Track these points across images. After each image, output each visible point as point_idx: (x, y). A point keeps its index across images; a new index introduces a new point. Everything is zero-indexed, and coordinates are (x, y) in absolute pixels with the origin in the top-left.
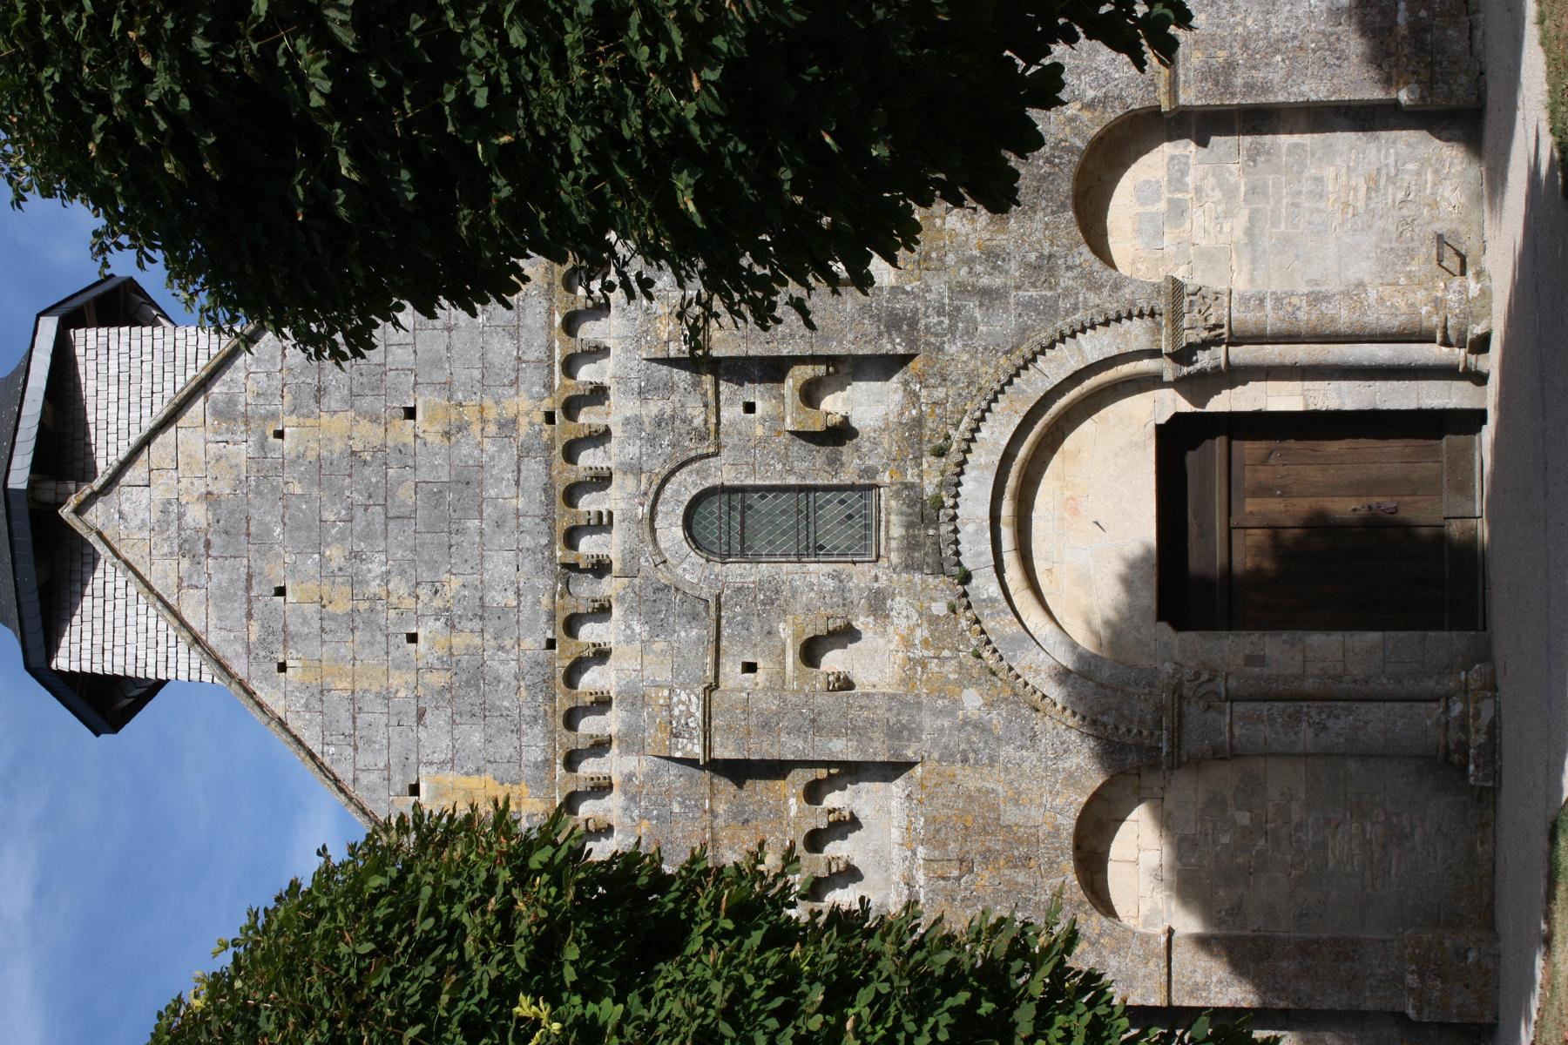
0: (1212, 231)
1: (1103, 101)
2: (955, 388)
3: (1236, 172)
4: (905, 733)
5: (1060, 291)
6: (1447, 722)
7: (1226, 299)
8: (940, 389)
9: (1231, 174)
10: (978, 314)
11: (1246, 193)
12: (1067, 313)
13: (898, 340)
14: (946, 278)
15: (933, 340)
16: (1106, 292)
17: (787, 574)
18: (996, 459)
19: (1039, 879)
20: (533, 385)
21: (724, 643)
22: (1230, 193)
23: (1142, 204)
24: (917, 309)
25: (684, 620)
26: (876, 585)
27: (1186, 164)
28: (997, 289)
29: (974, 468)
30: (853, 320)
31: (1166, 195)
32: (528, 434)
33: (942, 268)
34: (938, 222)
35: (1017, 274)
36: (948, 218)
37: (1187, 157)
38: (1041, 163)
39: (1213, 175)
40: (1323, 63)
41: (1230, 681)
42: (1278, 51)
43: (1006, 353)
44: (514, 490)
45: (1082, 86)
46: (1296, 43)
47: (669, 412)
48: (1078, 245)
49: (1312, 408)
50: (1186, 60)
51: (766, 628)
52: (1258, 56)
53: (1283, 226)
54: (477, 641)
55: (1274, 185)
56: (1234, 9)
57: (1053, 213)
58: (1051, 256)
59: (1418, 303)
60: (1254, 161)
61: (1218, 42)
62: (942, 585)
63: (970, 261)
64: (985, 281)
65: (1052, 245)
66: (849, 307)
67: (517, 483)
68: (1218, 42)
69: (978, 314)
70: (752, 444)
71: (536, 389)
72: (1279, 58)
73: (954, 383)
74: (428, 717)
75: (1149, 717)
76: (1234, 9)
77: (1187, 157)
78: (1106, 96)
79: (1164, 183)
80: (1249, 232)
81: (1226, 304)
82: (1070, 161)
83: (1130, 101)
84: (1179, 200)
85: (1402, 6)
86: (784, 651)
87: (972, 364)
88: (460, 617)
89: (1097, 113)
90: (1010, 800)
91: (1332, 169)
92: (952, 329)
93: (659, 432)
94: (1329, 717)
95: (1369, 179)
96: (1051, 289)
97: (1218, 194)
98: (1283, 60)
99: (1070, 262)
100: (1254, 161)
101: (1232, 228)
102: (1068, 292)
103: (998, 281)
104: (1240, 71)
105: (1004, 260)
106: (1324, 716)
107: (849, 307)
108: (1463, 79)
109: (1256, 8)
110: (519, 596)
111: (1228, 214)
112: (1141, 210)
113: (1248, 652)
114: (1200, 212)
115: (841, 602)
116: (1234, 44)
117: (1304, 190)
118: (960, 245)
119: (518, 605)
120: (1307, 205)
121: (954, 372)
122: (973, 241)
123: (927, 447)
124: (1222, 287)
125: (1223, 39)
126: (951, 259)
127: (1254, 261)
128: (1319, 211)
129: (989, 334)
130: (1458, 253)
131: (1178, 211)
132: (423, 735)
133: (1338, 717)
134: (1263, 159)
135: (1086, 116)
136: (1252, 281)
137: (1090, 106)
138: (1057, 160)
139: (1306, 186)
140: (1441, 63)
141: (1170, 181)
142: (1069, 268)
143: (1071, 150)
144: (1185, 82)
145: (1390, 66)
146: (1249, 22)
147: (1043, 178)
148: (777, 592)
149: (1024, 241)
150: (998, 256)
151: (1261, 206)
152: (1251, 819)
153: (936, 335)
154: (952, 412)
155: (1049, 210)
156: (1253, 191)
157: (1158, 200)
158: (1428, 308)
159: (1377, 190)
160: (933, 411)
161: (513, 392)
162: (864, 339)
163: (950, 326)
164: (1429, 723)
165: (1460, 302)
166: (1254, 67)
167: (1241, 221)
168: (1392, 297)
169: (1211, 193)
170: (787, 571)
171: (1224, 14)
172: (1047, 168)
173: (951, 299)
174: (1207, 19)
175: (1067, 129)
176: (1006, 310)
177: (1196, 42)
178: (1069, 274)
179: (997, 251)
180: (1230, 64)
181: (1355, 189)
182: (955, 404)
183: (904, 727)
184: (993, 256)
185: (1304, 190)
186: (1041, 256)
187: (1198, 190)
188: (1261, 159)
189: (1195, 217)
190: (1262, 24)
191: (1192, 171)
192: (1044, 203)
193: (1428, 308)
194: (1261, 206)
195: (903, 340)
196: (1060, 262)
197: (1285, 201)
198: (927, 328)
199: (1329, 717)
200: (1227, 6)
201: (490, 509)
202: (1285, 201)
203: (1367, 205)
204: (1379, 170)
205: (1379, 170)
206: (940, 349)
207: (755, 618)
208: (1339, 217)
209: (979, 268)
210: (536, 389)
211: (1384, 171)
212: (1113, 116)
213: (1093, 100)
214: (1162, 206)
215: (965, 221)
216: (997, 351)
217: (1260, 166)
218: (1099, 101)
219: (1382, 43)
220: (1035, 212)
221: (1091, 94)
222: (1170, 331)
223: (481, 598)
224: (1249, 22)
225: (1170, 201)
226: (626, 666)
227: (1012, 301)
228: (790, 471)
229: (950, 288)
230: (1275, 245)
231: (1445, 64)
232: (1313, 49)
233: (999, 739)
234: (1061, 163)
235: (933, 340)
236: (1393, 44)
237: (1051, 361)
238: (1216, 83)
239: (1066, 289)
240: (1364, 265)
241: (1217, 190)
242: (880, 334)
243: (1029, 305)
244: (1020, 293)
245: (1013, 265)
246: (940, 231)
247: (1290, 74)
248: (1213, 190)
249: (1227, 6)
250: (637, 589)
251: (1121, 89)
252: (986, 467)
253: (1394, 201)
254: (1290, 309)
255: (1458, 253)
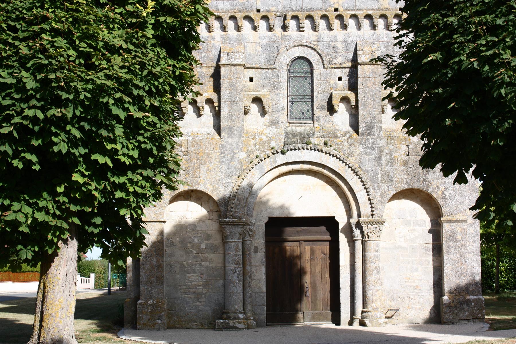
1: (444, 198)
2: (347, 149)
4: (230, 133)
5: (380, 184)
8: (347, 143)
10: (373, 156)
11: (413, 246)
13: (363, 129)
15: (364, 141)
16: (380, 199)
17: (283, 92)
20: (348, 4)
21: (260, 70)
25: (267, 57)
26: (280, 122)
28: (381, 163)
30: (370, 114)
33: (388, 144)
34: (404, 143)
35: (386, 169)
37: (425, 226)
38: (424, 177)
40: (457, 271)
41: (249, 241)
42: (461, 256)
43: (359, 166)
45: (449, 191)
46: (464, 262)
47: (338, 51)
48: (396, 190)
49: (341, 268)
51: (265, 85)
57: (407, 181)
59: (376, 303)
60: (423, 249)
61: (464, 236)
62: (280, 144)
64: (384, 159)
65: (396, 181)
66: (375, 112)
68: (464, 236)
69: (373, 156)
70: (328, 80)
72: (459, 256)
73: (349, 148)
75: (237, 214)
77: (425, 226)
81: (376, 239)
82: (424, 187)
83: (444, 207)
86: (257, 91)
87: (355, 154)
89: (440, 196)
92: (367, 148)
93: (332, 48)
94: (238, 274)
96: (381, 181)
99: (390, 187)
100: (423, 249)
103: (384, 163)
104: (454, 244)
105: (391, 165)
106: (238, 272)
107: (375, 112)
108: (451, 317)
109: (475, 249)
113: (259, 247)
115: (274, 110)
118: (396, 150)
121: (353, 149)
122: (397, 154)
124: (381, 238)
125: (465, 238)
126: (391, 147)
129: (366, 160)
130: (392, 316)
131: (407, 223)
133: (238, 277)
135: (440, 192)
137: (443, 194)
138: (424, 183)
140: (456, 310)
142: (388, 187)
143: (428, 187)
144: (451, 225)
145: (456, 293)
147: (418, 178)
150: (392, 163)
153: (365, 142)
154: (339, 148)
155: (408, 180)
159: (414, 289)
160: (339, 141)
163: (368, 147)
164: (236, 307)
166: (455, 248)
170: (284, 92)
171: (473, 238)
172: (422, 179)
173: (378, 147)
174: (471, 233)
175: (435, 186)
177: (464, 229)
178: (386, 187)
179: (394, 163)
183: (232, 132)
184: (392, 161)
185: (414, 265)
186: (392, 177)
187: (414, 230)
188: (424, 251)
190: (470, 251)
192: (410, 178)
195: (363, 131)
196: (390, 184)
198: (368, 139)
199: (238, 274)
204: (420, 290)
205: (420, 290)
206: (360, 143)
207: (268, 81)
209: (388, 156)
210: (346, 5)
212: (439, 201)
216: (360, 163)
217: (422, 250)
219: (463, 290)
222: (367, 221)
224: (470, 247)
226: (251, 37)
227: (377, 168)
229: (381, 147)
231: (456, 311)
233: (229, 164)
234: (423, 184)
235: (364, 141)
236: (463, 294)
238: (450, 236)
239: (381, 186)
242: (366, 123)
243: (375, 173)
246: (401, 143)
247: (453, 260)
250: (278, 40)
251: (448, 204)
253: (410, 295)
254: (374, 261)
255: (392, 316)
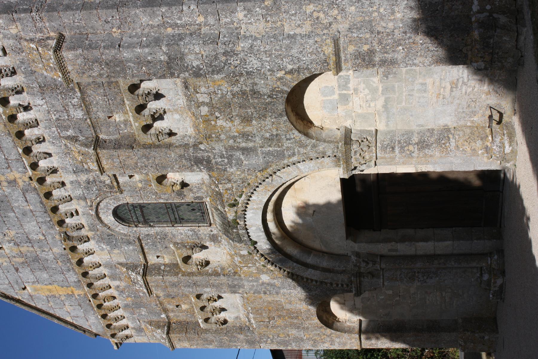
0: (364, 106)
1: (298, 70)
2: (236, 184)
3: (377, 82)
4: (237, 287)
5: (284, 148)
6: (481, 281)
7: (374, 149)
8: (228, 184)
9: (374, 82)
10: (242, 157)
11: (382, 91)
12: (290, 156)
13: (202, 168)
14: (222, 144)
15: (220, 167)
16: (309, 148)
17: (168, 230)
18: (262, 206)
19: (303, 322)
20: (18, 168)
21: (146, 251)
22: (374, 91)
23: (325, 96)
24: (210, 156)
25: (125, 244)
26: (212, 233)
27: (348, 79)
28: (251, 148)
29: (250, 209)
30: (176, 160)
31: (337, 92)
32: (24, 185)
33: (219, 139)
34: (213, 123)
35: (260, 142)
36: (218, 121)
37: (349, 76)
38: (266, 97)
39: (364, 83)
40: (427, 50)
41: (382, 265)
42: (401, 45)
43: (260, 171)
44: (26, 204)
45: (284, 64)
46: (411, 41)
47: (91, 179)
48: (291, 130)
49: (419, 171)
50: (345, 49)
51: (164, 246)
52: (388, 47)
53: (404, 104)
54: (32, 249)
55: (398, 86)
56: (371, 4)
57: (275, 117)
58: (277, 135)
59: (477, 149)
60: (387, 77)
61: (364, 41)
62: (244, 246)
63: (234, 138)
64: (243, 145)
65: (277, 130)
66: (173, 156)
67: (26, 201)
68: (364, 41)
69: (242, 157)
70: (138, 189)
71: (20, 169)
72: (401, 48)
73: (235, 182)
74: (20, 270)
75: (346, 280)
76: (371, 4)
77: (349, 76)
78: (299, 68)
79: (336, 88)
80: (385, 107)
81: (374, 151)
82: (282, 97)
83: (313, 70)
84: (345, 94)
85: (476, 2)
86: (174, 252)
87: (243, 175)
88: (20, 242)
89: (295, 76)
90: (287, 303)
91: (431, 79)
92: (230, 163)
93: (89, 186)
94: (427, 278)
95: (452, 83)
96: (279, 147)
97: (367, 91)
98: (403, 49)
99: (288, 137)
100: (387, 77)
101: (375, 105)
102: (288, 149)
103: (251, 145)
104: (377, 55)
105: (252, 137)
106: (425, 278)
107: (173, 156)
108: (510, 60)
109: (386, 3)
110: (44, 236)
111: (374, 99)
112: (324, 98)
113: (389, 248)
114: (357, 99)
115: (197, 238)
116: (373, 41)
117: (416, 89)
118: (227, 132)
119: (46, 238)
120: (417, 95)
121: (234, 178)
122: (234, 129)
123: (226, 204)
124: (373, 129)
125: (367, 39)
126: (223, 137)
127: (388, 118)
128: (424, 97)
129: (249, 164)
130: (499, 112)
131: (344, 99)
132: (21, 275)
133: (431, 278)
134: (392, 76)
135: (289, 77)
136: (387, 125)
137: (291, 72)
138: (274, 96)
139: (417, 87)
140: (498, 53)
141: (339, 86)
142: (287, 139)
143: (282, 92)
144: (345, 60)
145: (467, 50)
146: (382, 10)
147: (269, 103)
148: (166, 236)
149: (261, 130)
150: (249, 135)
151: (391, 96)
152: (393, 293)
153: (222, 165)
154: (236, 192)
155: (274, 117)
156: (386, 90)
157: (334, 93)
158: (483, 151)
159: (457, 87)
160: (227, 192)
161: (9, 171)
162: (184, 168)
163: (228, 162)
164: (473, 280)
165: (500, 152)
166: (386, 53)
167: (380, 102)
168: (463, 145)
169: (363, 91)
170: (169, 230)
171: (366, 6)
172: (269, 100)
173: (226, 152)
174: (356, 9)
175: (279, 83)
176: (257, 155)
177: (350, 41)
178: (289, 141)
179: (248, 133)
180: (371, 51)
181: (444, 88)
182: (237, 189)
183: (236, 285)
184: (245, 136)
185: (416, 89)
186: (272, 135)
187: (356, 90)
188: (390, 76)
189: (354, 101)
190: (389, 11)
191: (351, 82)
192: (270, 114)
193: (483, 151)
194: (391, 96)
195: (205, 167)
196: (283, 137)
197: (404, 94)
198: (217, 163)
199: (427, 278)
200: (368, 2)
201: (17, 210)
202: (404, 94)
203: (451, 94)
204: (458, 80)
205: (458, 80)
206: (225, 170)
207: (158, 243)
208: (435, 100)
209: (239, 140)
210: (20, 169)
211: (461, 80)
212: (304, 77)
213: (292, 70)
214: (336, 97)
215: (227, 122)
216: (255, 171)
217: (390, 79)
218: (295, 71)
219: (463, 40)
220: (266, 118)
221: (290, 67)
222: (345, 166)
223: (27, 237)
224: (382, 10)
225: (340, 95)
226: (103, 257)
227: (259, 152)
228: (160, 198)
229: (225, 148)
230: (399, 111)
231: (500, 53)
232: (421, 44)
233: (279, 287)
234: (277, 97)
235: (220, 167)
236: (469, 40)
237: (284, 173)
238: (364, 60)
239: (288, 147)
240: (448, 118)
241: (366, 90)
242: (192, 165)
243: (269, 153)
244: (263, 149)
245: (257, 139)
246: (215, 126)
247: (407, 56)
248: (364, 90)
249: (368, 2)
250: (99, 235)
251: (308, 65)
252: (257, 209)
253: (466, 92)
254: (408, 153)
255: (499, 112)
